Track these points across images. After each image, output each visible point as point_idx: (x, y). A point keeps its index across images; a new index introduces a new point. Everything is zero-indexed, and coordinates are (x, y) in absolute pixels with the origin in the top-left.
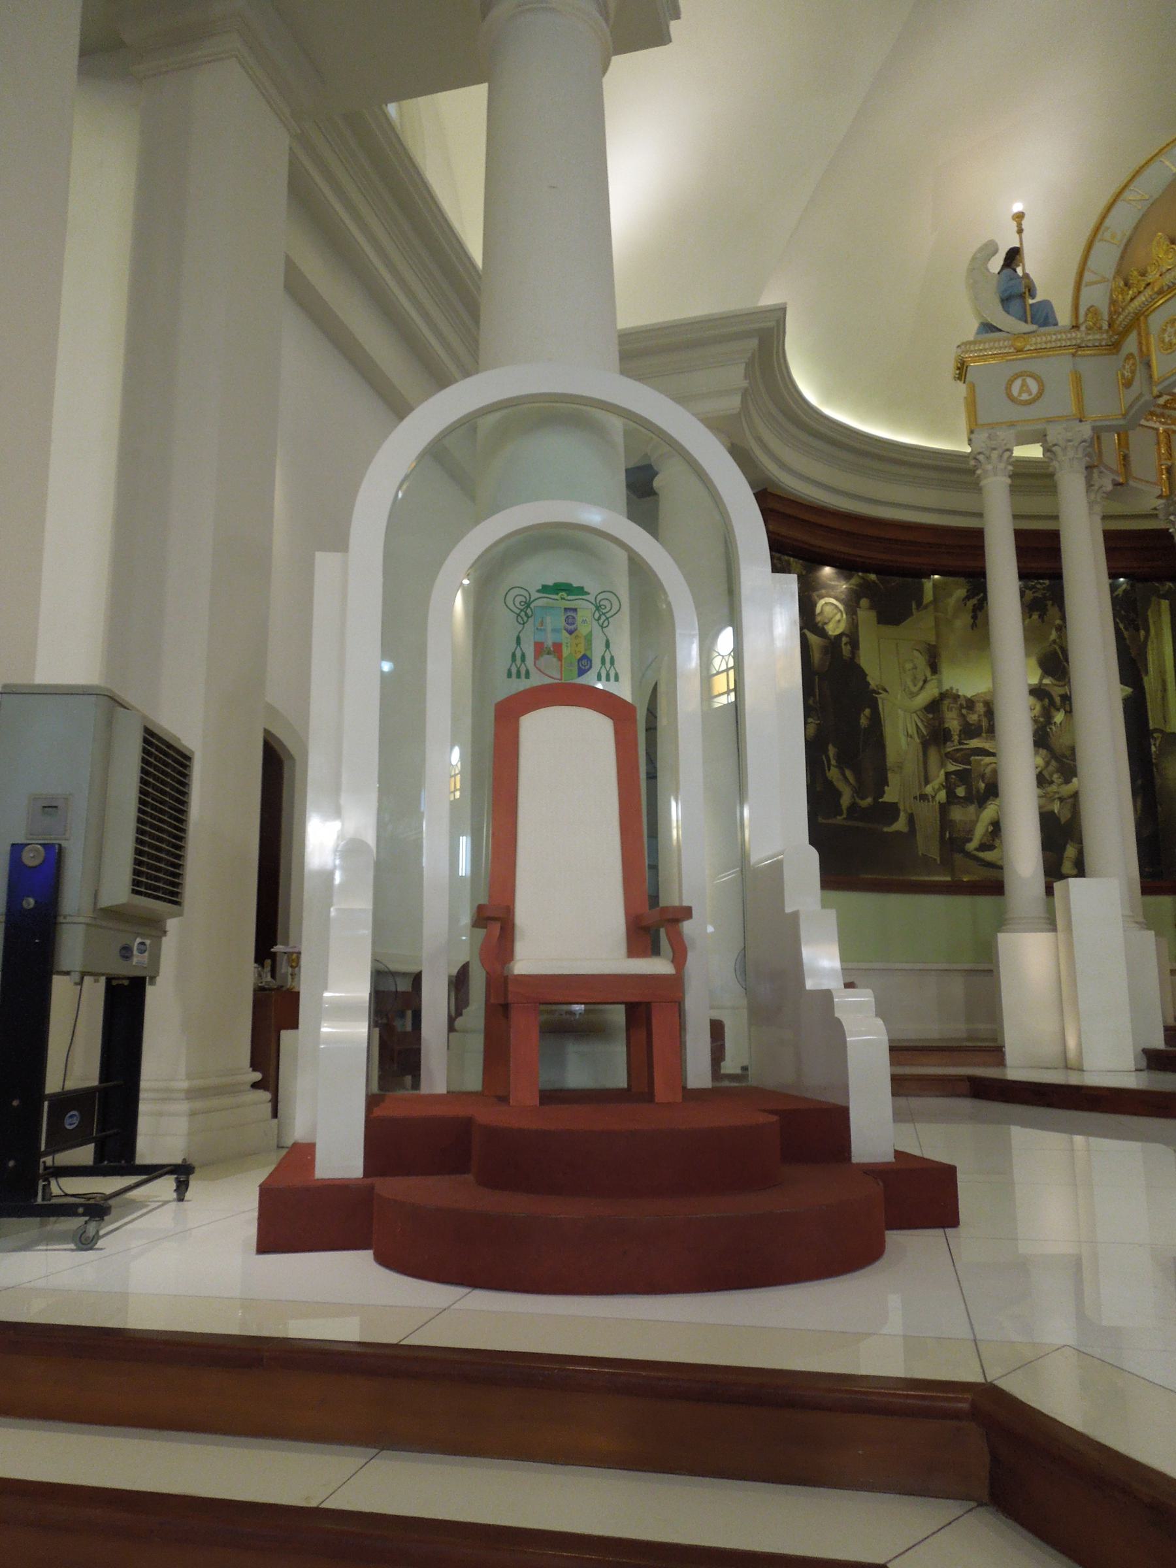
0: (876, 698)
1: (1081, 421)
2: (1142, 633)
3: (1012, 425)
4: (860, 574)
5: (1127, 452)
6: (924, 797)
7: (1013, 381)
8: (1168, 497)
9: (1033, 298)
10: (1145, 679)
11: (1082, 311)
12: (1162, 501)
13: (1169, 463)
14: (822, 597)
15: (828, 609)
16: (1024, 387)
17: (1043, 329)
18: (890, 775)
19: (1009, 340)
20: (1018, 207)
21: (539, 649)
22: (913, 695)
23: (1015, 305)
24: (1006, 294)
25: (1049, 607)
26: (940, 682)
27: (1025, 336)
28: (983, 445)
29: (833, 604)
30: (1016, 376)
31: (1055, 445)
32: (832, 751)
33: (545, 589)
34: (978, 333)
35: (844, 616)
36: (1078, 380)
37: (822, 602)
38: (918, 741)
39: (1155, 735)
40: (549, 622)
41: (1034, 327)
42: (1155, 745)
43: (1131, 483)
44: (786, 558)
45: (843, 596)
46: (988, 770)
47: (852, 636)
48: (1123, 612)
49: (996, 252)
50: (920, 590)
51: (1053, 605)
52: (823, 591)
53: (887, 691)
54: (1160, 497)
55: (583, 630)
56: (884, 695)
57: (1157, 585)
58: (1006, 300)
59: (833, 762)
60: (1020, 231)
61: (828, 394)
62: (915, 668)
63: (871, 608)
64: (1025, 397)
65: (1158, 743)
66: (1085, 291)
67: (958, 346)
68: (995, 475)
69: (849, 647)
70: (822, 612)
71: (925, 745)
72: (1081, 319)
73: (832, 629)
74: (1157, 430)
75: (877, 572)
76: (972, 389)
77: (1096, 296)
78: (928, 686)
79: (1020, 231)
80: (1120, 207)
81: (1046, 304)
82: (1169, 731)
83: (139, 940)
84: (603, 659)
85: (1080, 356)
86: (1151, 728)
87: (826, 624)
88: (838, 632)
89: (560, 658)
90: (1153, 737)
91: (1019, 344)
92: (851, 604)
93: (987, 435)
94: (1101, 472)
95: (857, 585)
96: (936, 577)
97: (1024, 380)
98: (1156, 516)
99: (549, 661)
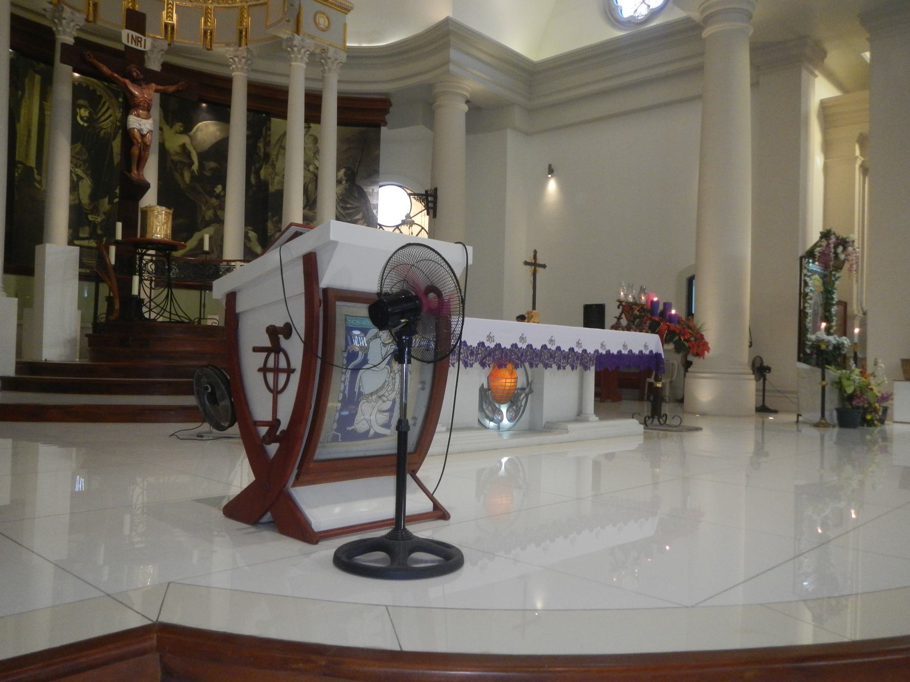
8: (55, 5)
10: (18, 126)
12: (51, 6)
39: (19, 165)
42: (17, 172)
54: (51, 3)
57: (35, 63)
65: (20, 171)
82: (28, 164)
86: (17, 159)
90: (17, 167)
98: (44, 16)
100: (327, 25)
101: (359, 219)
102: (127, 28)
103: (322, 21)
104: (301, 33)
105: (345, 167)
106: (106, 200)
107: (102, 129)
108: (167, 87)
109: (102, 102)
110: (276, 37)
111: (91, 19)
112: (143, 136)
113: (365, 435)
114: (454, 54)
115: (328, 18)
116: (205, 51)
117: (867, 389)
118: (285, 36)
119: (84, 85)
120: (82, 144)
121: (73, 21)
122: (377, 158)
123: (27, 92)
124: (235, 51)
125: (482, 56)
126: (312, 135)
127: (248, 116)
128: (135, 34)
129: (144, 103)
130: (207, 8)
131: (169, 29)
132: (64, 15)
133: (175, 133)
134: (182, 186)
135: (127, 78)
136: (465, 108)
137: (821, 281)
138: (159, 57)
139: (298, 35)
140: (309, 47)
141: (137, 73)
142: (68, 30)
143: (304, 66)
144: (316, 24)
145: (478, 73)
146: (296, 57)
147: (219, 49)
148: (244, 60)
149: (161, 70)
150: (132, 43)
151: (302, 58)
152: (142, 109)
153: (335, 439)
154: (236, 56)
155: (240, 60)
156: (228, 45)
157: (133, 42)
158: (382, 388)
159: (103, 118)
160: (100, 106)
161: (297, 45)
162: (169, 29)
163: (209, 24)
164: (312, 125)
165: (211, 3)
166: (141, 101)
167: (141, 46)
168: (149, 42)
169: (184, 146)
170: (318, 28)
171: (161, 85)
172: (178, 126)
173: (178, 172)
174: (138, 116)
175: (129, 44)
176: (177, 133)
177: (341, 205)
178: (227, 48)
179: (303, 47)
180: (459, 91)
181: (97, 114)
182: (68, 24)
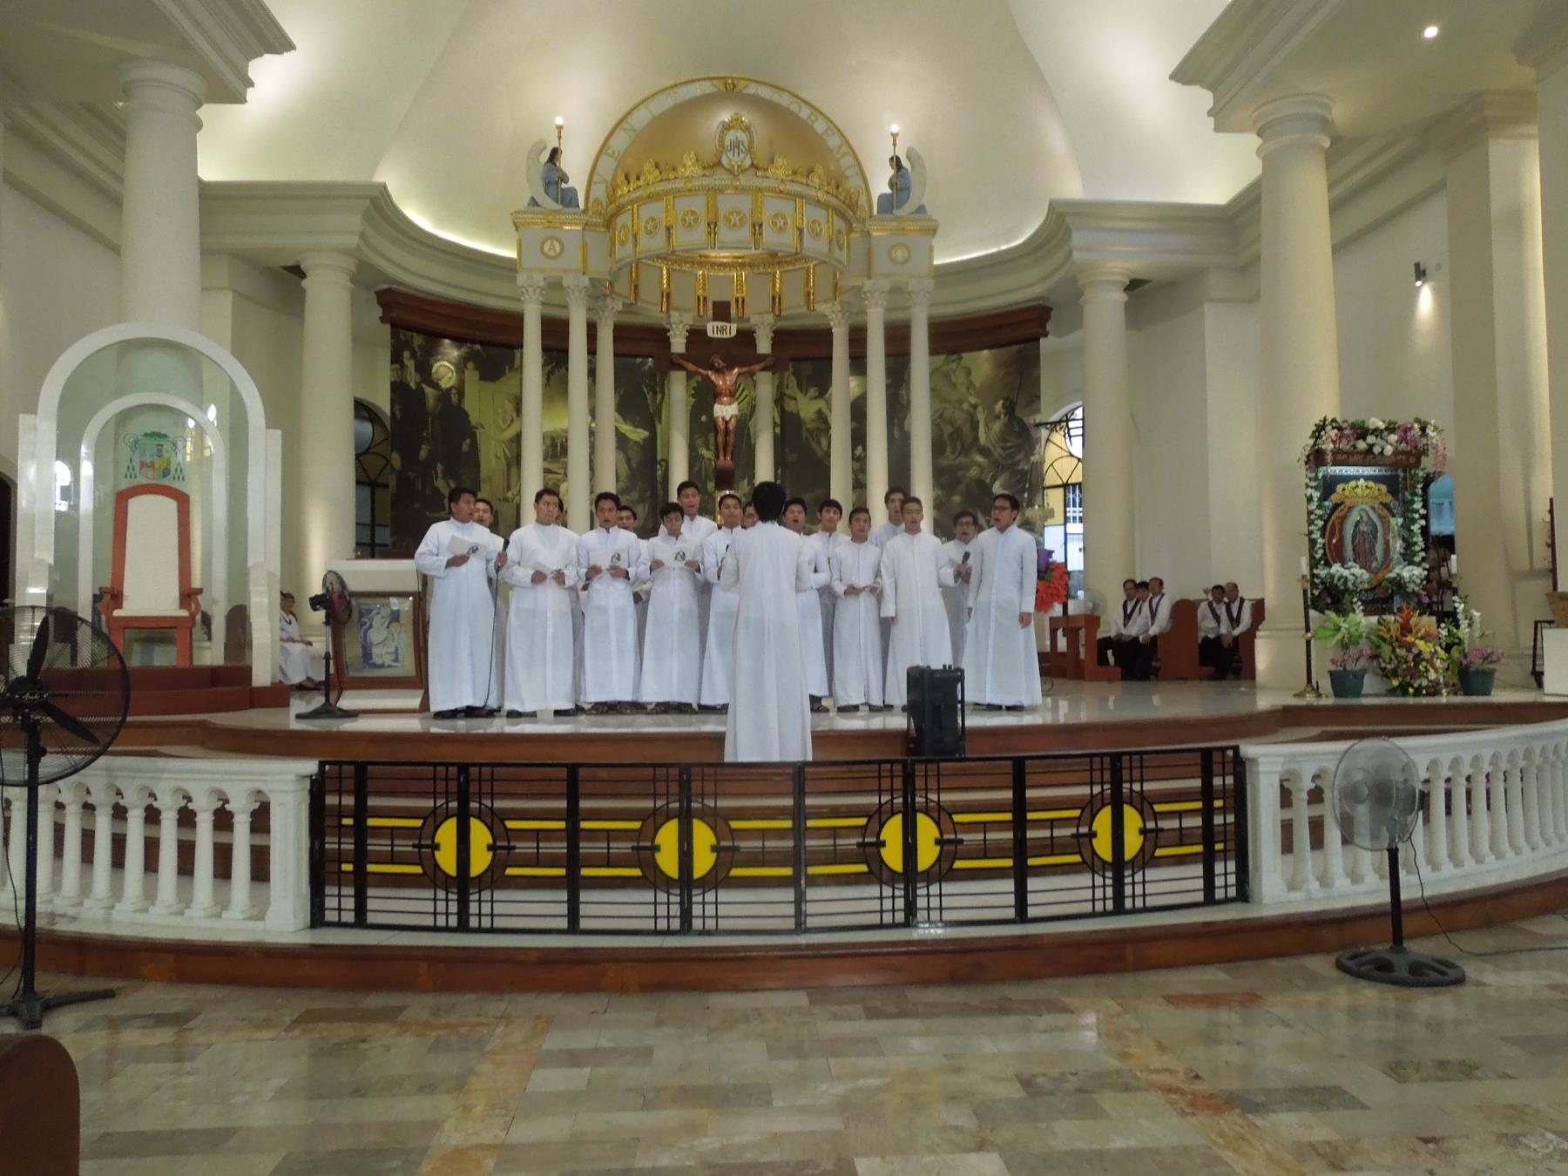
0: (475, 434)
1: (584, 274)
2: (659, 396)
3: (542, 271)
4: (469, 345)
6: (506, 500)
9: (567, 182)
10: (659, 427)
11: (591, 200)
14: (439, 360)
15: (442, 370)
16: (552, 248)
18: (482, 485)
19: (541, 213)
20: (559, 121)
21: (143, 465)
22: (504, 430)
23: (552, 188)
30: (547, 239)
32: (439, 467)
33: (146, 435)
34: (529, 205)
36: (584, 247)
37: (438, 364)
38: (503, 461)
40: (148, 453)
41: (561, 207)
43: (639, 304)
44: (409, 333)
45: (454, 361)
46: (550, 483)
47: (460, 389)
49: (545, 148)
50: (514, 354)
52: (439, 357)
53: (482, 427)
55: (166, 455)
56: (481, 429)
59: (440, 475)
60: (560, 137)
61: (441, 222)
62: (505, 412)
64: (552, 253)
66: (593, 186)
71: (509, 466)
72: (590, 205)
74: (662, 269)
75: (481, 343)
77: (599, 192)
78: (514, 425)
79: (560, 137)
80: (619, 133)
81: (573, 191)
84: (176, 470)
86: (659, 458)
88: (449, 385)
89: (154, 468)
91: (550, 218)
92: (461, 367)
99: (150, 473)
100: (906, 254)
101: (1019, 461)
102: (715, 318)
103: (900, 254)
105: (1003, 398)
106: (746, 481)
110: (853, 287)
111: (702, 313)
112: (727, 422)
113: (382, 666)
114: (1077, 238)
117: (1383, 644)
118: (860, 284)
121: (681, 322)
122: (1039, 375)
123: (666, 396)
125: (1127, 225)
126: (964, 367)
127: (887, 363)
128: (720, 324)
132: (672, 320)
134: (820, 454)
135: (711, 369)
136: (1123, 297)
137: (1384, 488)
139: (869, 278)
142: (678, 333)
144: (893, 260)
145: (1124, 249)
148: (840, 315)
152: (726, 396)
153: (365, 667)
154: (833, 312)
158: (386, 639)
164: (964, 355)
169: (819, 412)
171: (746, 366)
172: (813, 391)
173: (814, 440)
174: (722, 403)
175: (715, 336)
176: (811, 399)
177: (1001, 444)
180: (1105, 278)
182: (678, 327)
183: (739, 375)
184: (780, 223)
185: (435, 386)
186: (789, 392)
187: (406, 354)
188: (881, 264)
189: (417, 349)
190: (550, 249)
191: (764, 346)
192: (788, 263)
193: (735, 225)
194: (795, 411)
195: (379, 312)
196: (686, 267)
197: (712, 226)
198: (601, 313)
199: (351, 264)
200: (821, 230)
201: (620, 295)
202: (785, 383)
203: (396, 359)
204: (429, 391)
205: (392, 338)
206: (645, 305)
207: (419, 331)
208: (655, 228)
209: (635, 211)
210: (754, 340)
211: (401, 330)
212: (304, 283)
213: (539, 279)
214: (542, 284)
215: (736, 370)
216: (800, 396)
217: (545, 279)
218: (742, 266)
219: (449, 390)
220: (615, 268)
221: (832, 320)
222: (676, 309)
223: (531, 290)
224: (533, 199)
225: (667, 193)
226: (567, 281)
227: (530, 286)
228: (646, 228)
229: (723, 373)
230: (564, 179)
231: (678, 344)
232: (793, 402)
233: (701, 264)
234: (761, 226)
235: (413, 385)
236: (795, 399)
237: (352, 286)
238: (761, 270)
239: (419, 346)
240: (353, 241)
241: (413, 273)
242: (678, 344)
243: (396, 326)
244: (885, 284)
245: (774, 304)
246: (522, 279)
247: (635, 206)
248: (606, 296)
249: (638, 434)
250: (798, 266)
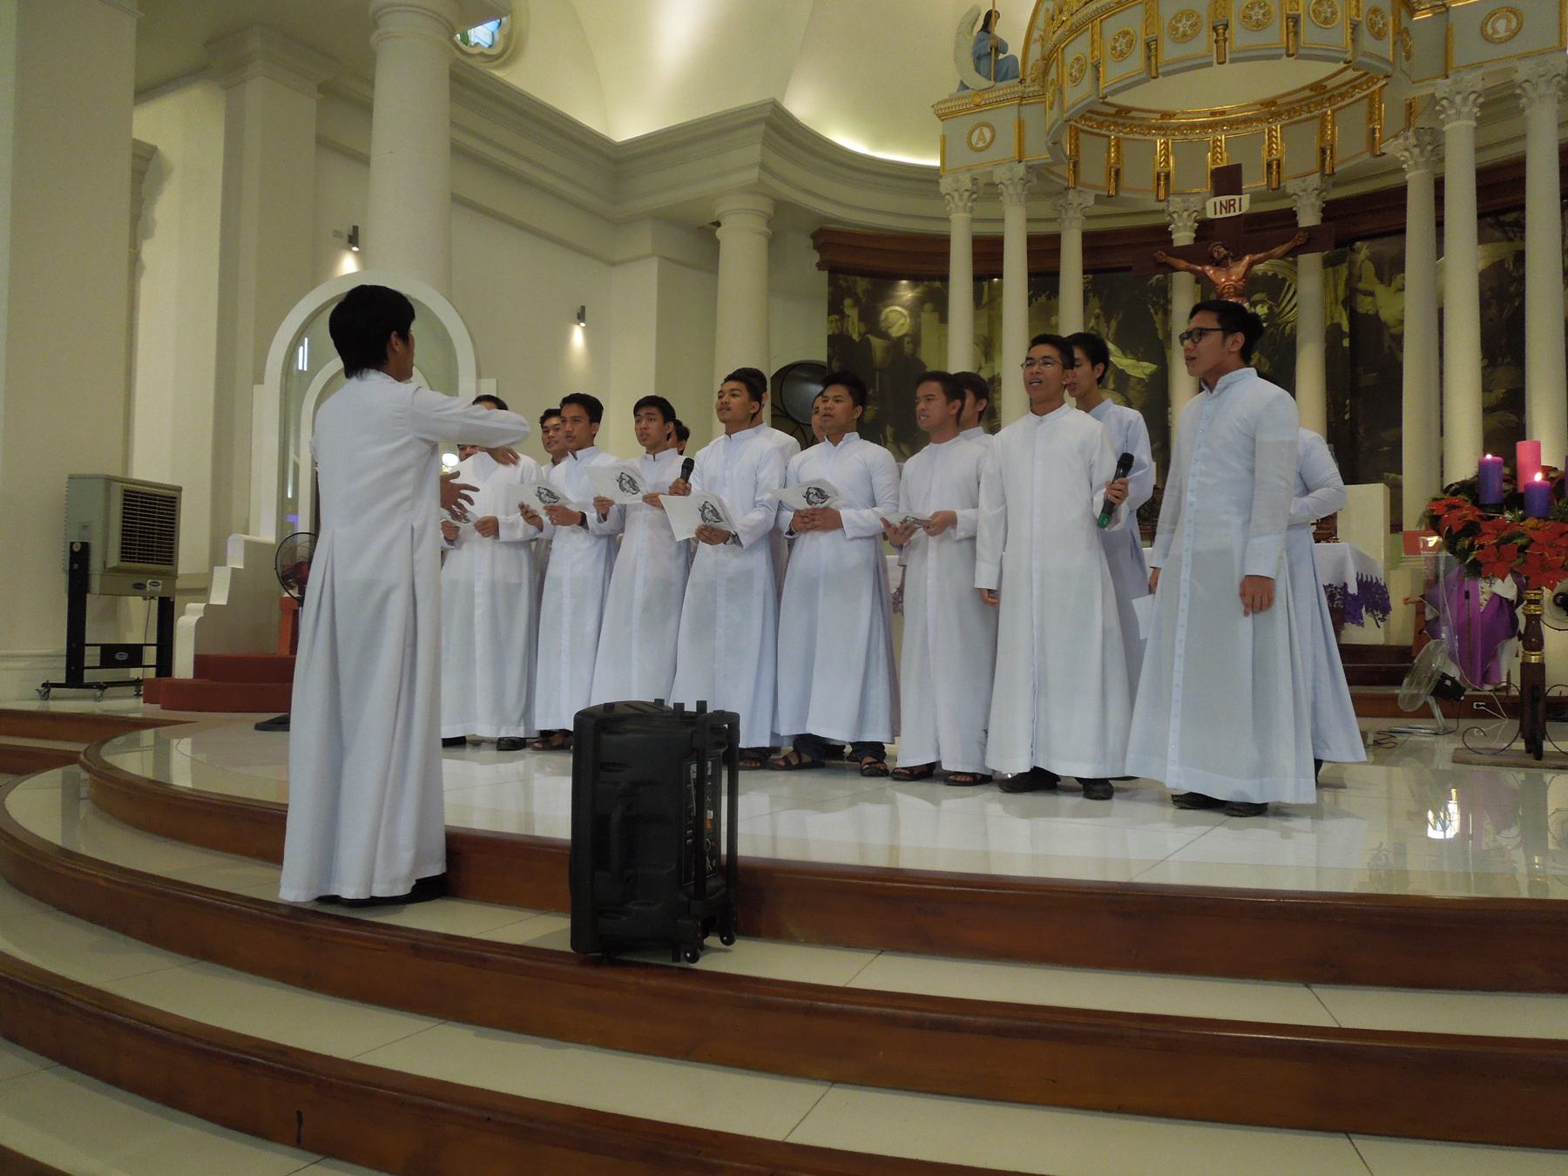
1: (1020, 162)
4: (926, 283)
5: (1118, 166)
7: (974, 130)
9: (1005, 53)
13: (1166, 170)
14: (887, 306)
15: (893, 316)
17: (1000, 84)
23: (984, 62)
24: (977, 55)
25: (1090, 299)
26: (993, 368)
27: (980, 93)
28: (949, 187)
29: (897, 311)
31: (1001, 183)
34: (958, 90)
35: (908, 320)
36: (1021, 125)
41: (992, 83)
43: (1122, 194)
44: (853, 278)
45: (908, 303)
47: (915, 337)
48: (1155, 299)
49: (979, 15)
51: (1094, 296)
52: (889, 301)
58: (978, 58)
61: (879, 141)
63: (934, 310)
64: (981, 145)
67: (933, 106)
68: (957, 212)
69: (911, 346)
70: (886, 319)
73: (896, 332)
76: (944, 140)
77: (1036, 52)
81: (1014, 58)
83: (149, 581)
85: (1025, 104)
87: (890, 328)
88: (901, 333)
91: (977, 100)
92: (916, 309)
93: (950, 179)
94: (1081, 191)
95: (921, 293)
96: (996, 279)
97: (981, 130)
100: (1514, 22)
102: (1218, 192)
103: (1501, 26)
104: (1450, 72)
107: (1289, 322)
108: (1273, 251)
109: (1287, 284)
115: (1515, 14)
116: (1379, 159)
118: (1431, 90)
119: (1270, 274)
120: (1260, 353)
121: (1186, 210)
124: (1407, 138)
129: (1229, 288)
130: (1374, 92)
131: (1328, 152)
133: (1395, 292)
135: (1210, 264)
138: (1313, 199)
139: (1447, 77)
140: (1472, 86)
141: (1218, 252)
142: (1180, 224)
143: (1473, 123)
146: (1448, 116)
147: (1393, 148)
148: (1416, 151)
149: (1323, 220)
150: (1221, 213)
151: (1459, 113)
154: (1406, 150)
155: (1411, 153)
156: (1396, 136)
157: (1224, 211)
159: (1288, 309)
160: (1283, 295)
161: (1446, 95)
162: (1328, 152)
163: (1274, 152)
165: (1376, 83)
166: (1224, 288)
167: (1235, 211)
168: (1246, 198)
170: (1494, 43)
171: (1260, 252)
175: (1219, 216)
178: (1396, 143)
179: (1459, 93)
181: (1279, 306)
183: (1251, 264)
184: (1257, 14)
185: (884, 335)
186: (1361, 286)
187: (848, 302)
188: (1467, 48)
189: (862, 297)
190: (979, 139)
191: (1309, 218)
192: (1343, 96)
193: (1184, 35)
194: (1371, 312)
195: (816, 257)
196: (1194, 136)
197: (1151, 47)
198: (1063, 212)
199: (765, 205)
200: (1334, 13)
201: (1093, 187)
202: (1356, 272)
203: (835, 308)
204: (877, 343)
205: (829, 285)
206: (1128, 195)
207: (863, 274)
208: (1081, 71)
209: (1060, 57)
210: (1296, 215)
211: (841, 276)
212: (719, 233)
213: (966, 181)
214: (969, 185)
215: (1247, 258)
216: (1380, 290)
217: (974, 180)
218: (1277, 115)
219: (901, 338)
220: (1050, 144)
221: (1404, 162)
222: (1176, 194)
223: (956, 195)
224: (962, 82)
225: (1091, 19)
226: (1000, 175)
227: (956, 190)
228: (1071, 74)
229: (1226, 266)
230: (1000, 47)
231: (1183, 236)
232: (1369, 299)
233: (1213, 126)
234: (1226, 26)
235: (855, 337)
236: (1371, 294)
237: (767, 230)
238: (1305, 116)
239: (866, 292)
240: (753, 175)
241: (826, 199)
242: (1183, 236)
243: (834, 270)
244: (1474, 80)
245: (1323, 161)
246: (946, 184)
247: (1060, 50)
248: (1067, 189)
249: (1139, 369)
250: (1358, 96)
